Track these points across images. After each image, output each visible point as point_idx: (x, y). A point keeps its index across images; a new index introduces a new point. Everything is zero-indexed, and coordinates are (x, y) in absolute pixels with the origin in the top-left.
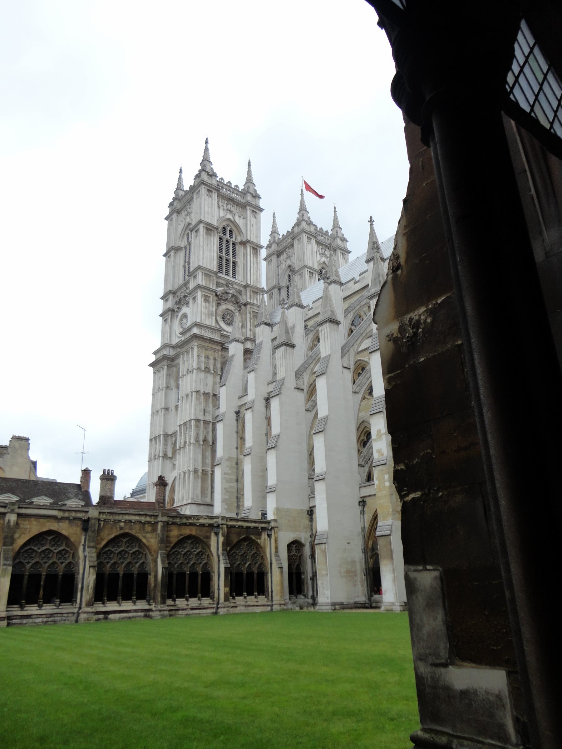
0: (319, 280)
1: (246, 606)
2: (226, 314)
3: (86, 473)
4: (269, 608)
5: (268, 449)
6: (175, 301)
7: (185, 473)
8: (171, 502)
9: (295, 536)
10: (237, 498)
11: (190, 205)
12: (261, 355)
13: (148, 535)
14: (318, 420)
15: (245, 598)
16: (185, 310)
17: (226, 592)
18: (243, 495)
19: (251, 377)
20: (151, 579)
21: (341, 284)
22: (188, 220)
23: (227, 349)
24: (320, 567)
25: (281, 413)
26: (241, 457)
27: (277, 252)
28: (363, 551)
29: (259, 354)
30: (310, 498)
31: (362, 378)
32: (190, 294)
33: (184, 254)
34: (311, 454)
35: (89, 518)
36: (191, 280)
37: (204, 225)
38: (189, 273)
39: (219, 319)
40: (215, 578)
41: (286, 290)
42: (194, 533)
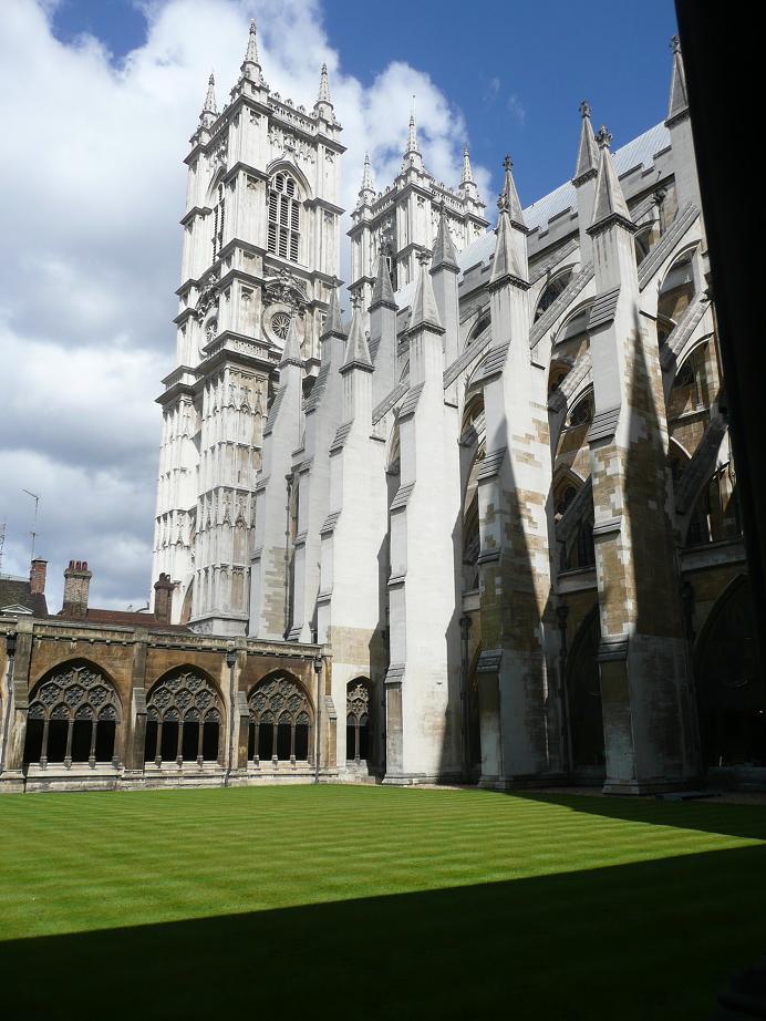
1: (275, 775)
3: (39, 566)
7: (206, 570)
9: (361, 670)
13: (117, 663)
15: (275, 762)
16: (212, 312)
20: (120, 730)
35: (16, 634)
39: (267, 327)
42: (193, 662)
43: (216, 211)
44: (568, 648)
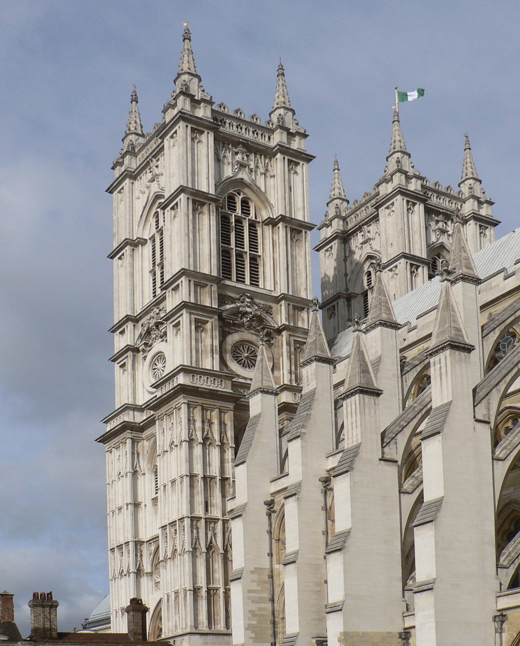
0: (431, 277)
5: (327, 553)
6: (137, 334)
11: (158, 161)
12: (312, 412)
16: (158, 346)
18: (283, 618)
21: (477, 281)
22: (155, 188)
23: (246, 408)
27: (343, 234)
29: (308, 410)
32: (167, 320)
33: (151, 251)
34: (407, 556)
36: (167, 294)
43: (153, 239)
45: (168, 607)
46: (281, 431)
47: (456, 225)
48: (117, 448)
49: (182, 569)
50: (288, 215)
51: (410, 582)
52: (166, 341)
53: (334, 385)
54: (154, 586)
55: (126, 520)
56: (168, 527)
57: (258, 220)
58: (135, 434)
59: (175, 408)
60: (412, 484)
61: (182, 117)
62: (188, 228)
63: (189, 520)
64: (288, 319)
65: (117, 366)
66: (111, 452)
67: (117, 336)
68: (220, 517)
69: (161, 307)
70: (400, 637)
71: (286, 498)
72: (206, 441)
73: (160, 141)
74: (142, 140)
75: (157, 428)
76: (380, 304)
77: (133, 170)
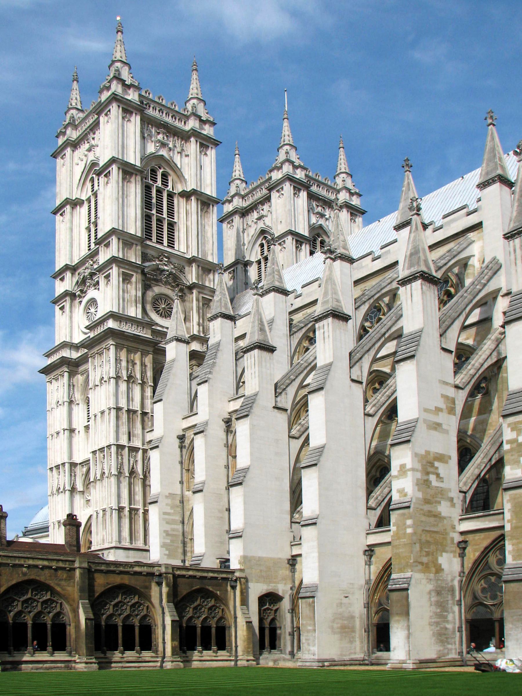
2: (157, 302)
4: (233, 663)
6: (75, 280)
8: (85, 544)
10: (184, 543)
11: (94, 134)
12: (217, 360)
14: (310, 449)
16: (91, 293)
17: (173, 645)
19: (203, 391)
22: (91, 157)
23: (163, 352)
24: (304, 622)
25: (252, 440)
26: (188, 494)
28: (366, 605)
29: (214, 359)
30: (292, 545)
31: (380, 396)
33: (87, 210)
36: (100, 249)
37: (120, 166)
38: (96, 239)
40: (160, 631)
41: (257, 266)
44: (467, 571)
45: (97, 522)
46: (191, 374)
47: (335, 212)
48: (57, 380)
49: (109, 491)
50: (199, 190)
51: (296, 516)
52: (99, 289)
53: (235, 338)
54: (85, 503)
55: (62, 442)
56: (98, 452)
57: (174, 192)
58: (72, 368)
59: (105, 348)
60: (299, 431)
61: (115, 98)
62: (118, 194)
63: (115, 447)
64: (198, 278)
65: (57, 308)
66: (51, 383)
67: (58, 282)
68: (140, 446)
69: (95, 260)
70: (288, 563)
71: (195, 434)
72: (130, 379)
73: (96, 116)
74: (81, 115)
75: (89, 366)
76: (274, 272)
77: (73, 140)
